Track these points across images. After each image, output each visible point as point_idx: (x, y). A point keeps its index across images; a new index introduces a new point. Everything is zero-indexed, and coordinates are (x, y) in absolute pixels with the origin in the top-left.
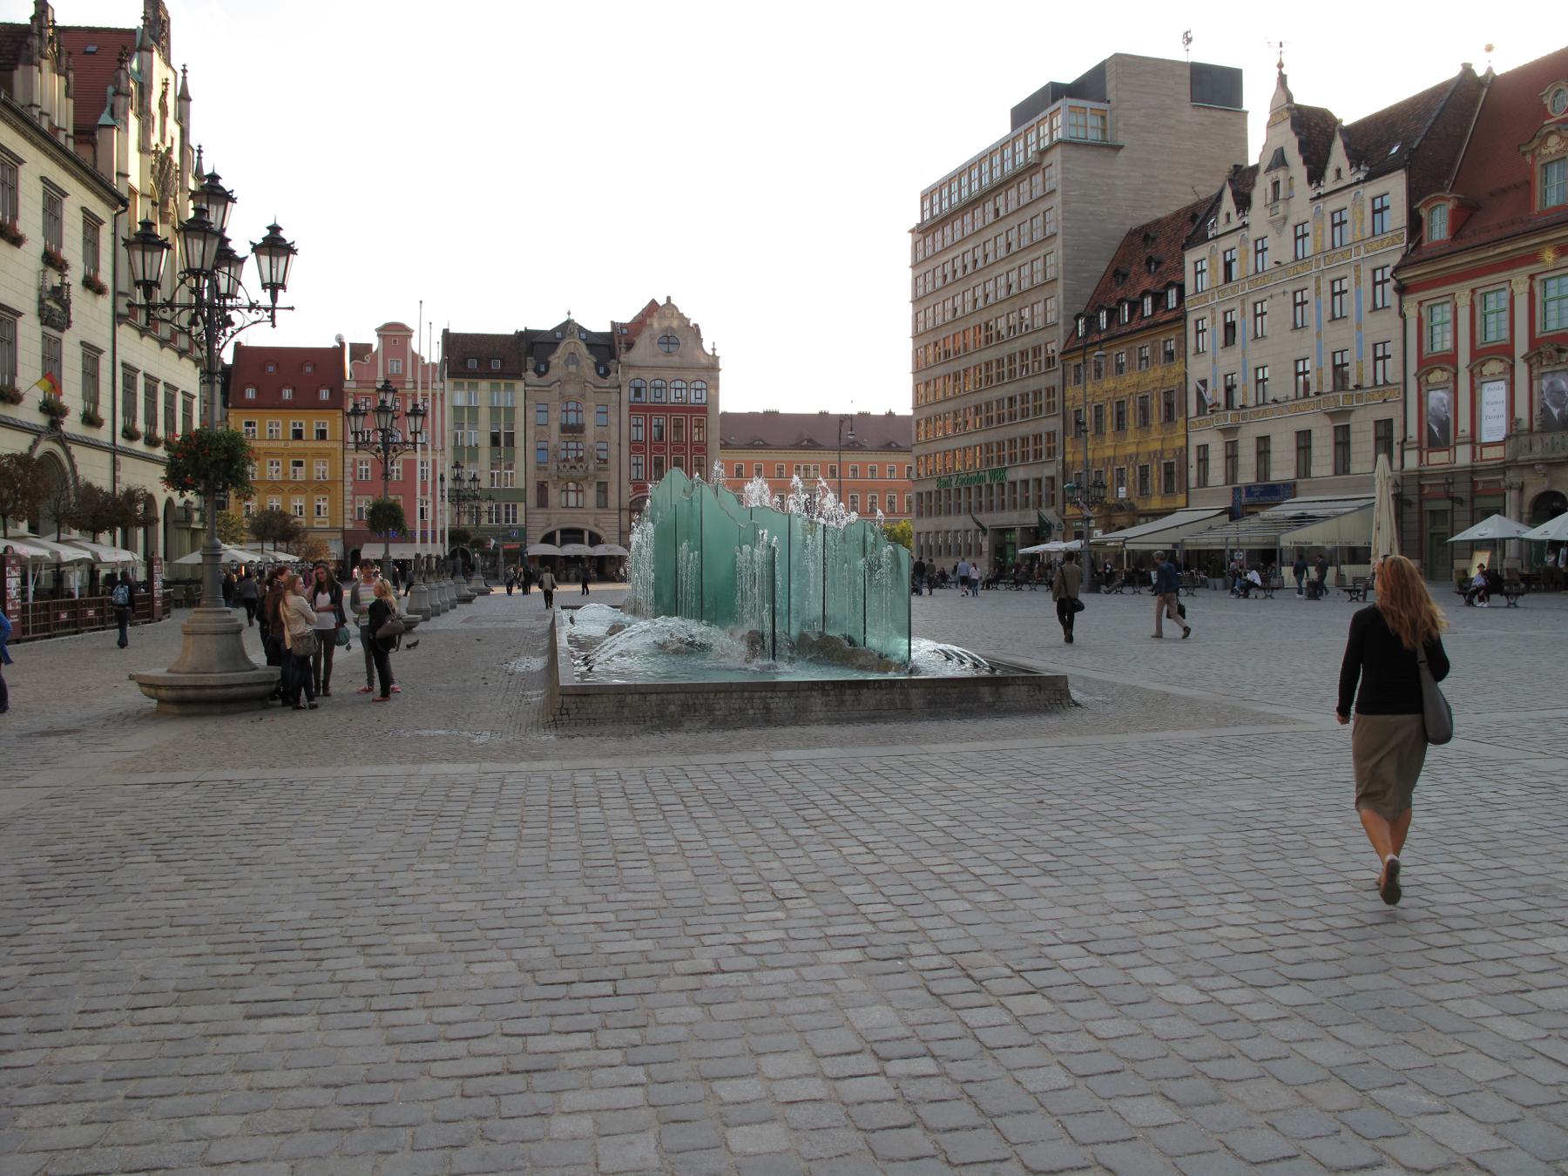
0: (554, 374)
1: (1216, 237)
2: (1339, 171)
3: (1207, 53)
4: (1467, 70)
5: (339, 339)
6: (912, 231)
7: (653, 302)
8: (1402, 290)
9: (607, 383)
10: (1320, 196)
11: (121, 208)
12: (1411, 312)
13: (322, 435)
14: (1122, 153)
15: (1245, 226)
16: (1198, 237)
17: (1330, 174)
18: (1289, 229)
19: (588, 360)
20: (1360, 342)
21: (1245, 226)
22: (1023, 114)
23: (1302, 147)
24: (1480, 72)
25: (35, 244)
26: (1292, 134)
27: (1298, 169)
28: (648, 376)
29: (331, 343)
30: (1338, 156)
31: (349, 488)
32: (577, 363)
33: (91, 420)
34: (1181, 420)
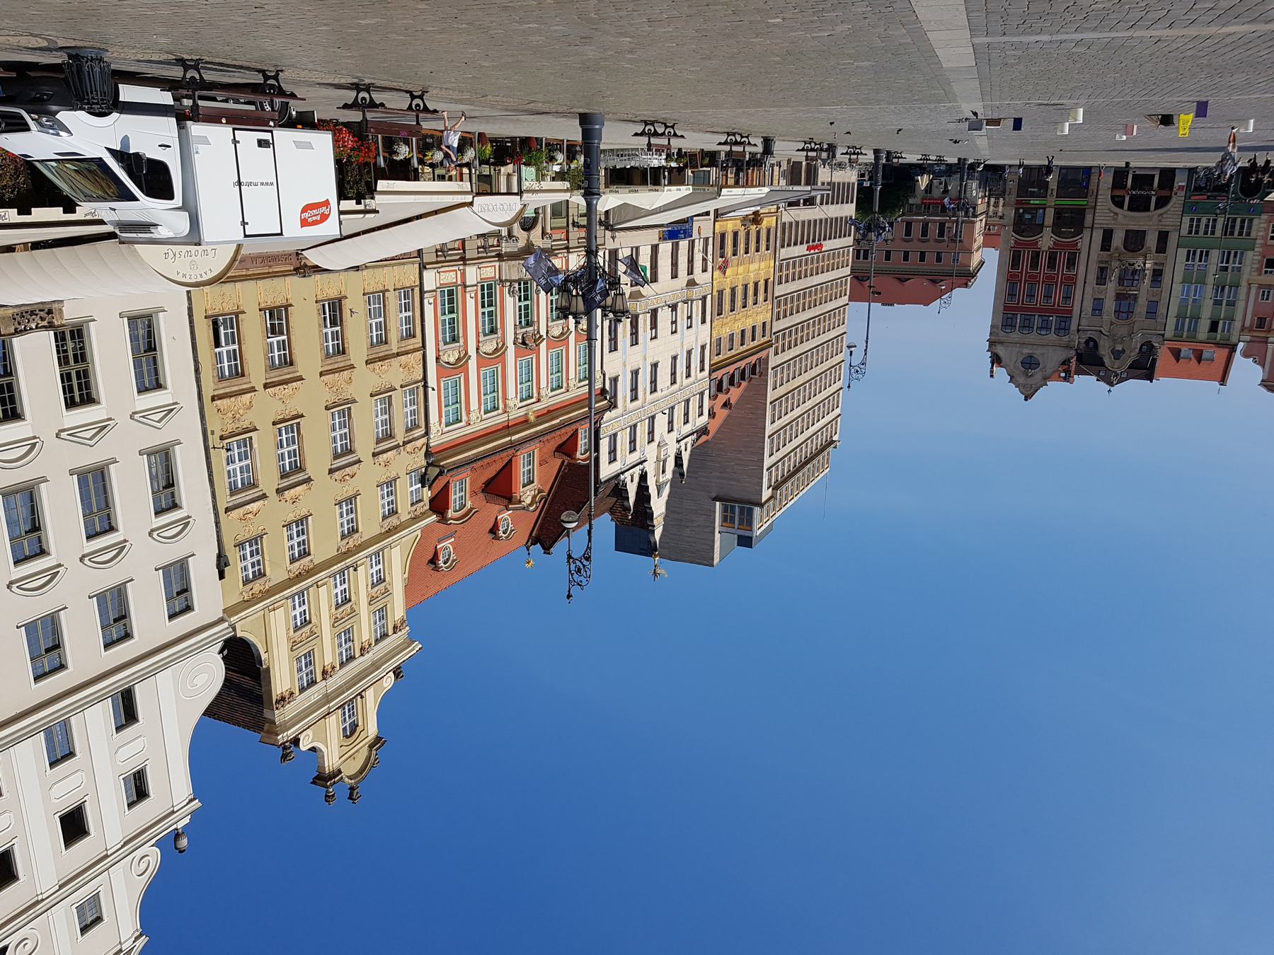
9: (1089, 334)
10: (641, 463)
14: (714, 495)
15: (678, 441)
17: (636, 479)
19: (1104, 351)
20: (625, 353)
28: (1052, 337)
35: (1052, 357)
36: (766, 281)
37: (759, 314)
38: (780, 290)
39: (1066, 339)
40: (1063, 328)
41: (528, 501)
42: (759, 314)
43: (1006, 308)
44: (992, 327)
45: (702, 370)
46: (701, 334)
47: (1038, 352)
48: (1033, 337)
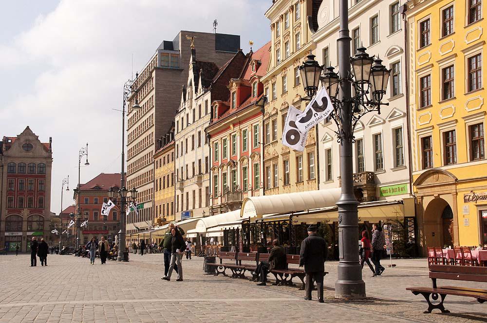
15: (185, 108)
28: (17, 162)
35: (15, 151)
36: (157, 190)
37: (161, 172)
38: (151, 186)
39: (9, 161)
40: (11, 167)
41: (234, 84)
42: (161, 172)
43: (44, 177)
45: (178, 145)
46: (180, 163)
47: (24, 154)
48: (28, 161)
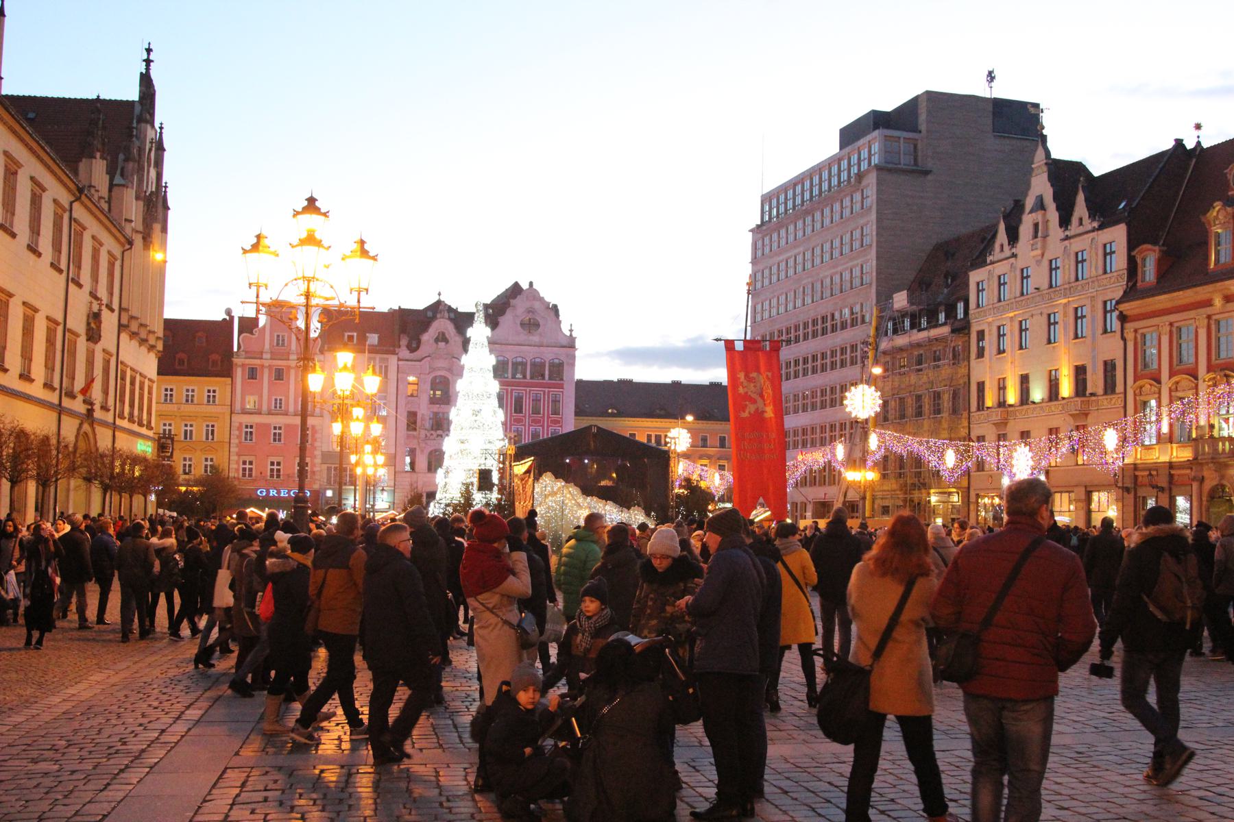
0: (424, 349)
1: (992, 263)
2: (1081, 219)
3: (1004, 90)
4: (1179, 143)
5: (228, 312)
6: (751, 231)
7: (516, 285)
8: (1123, 318)
10: (1067, 238)
11: (127, 247)
12: (1130, 336)
13: (211, 399)
14: (929, 177)
16: (980, 261)
17: (1075, 220)
18: (1045, 263)
21: (1014, 256)
22: (849, 135)
23: (1056, 198)
24: (1190, 144)
25: (87, 287)
26: (1048, 184)
27: (1053, 215)
29: (219, 316)
30: (1080, 208)
31: (234, 450)
32: (446, 341)
33: (105, 408)
34: (965, 414)
44: (573, 365)
47: (523, 337)
